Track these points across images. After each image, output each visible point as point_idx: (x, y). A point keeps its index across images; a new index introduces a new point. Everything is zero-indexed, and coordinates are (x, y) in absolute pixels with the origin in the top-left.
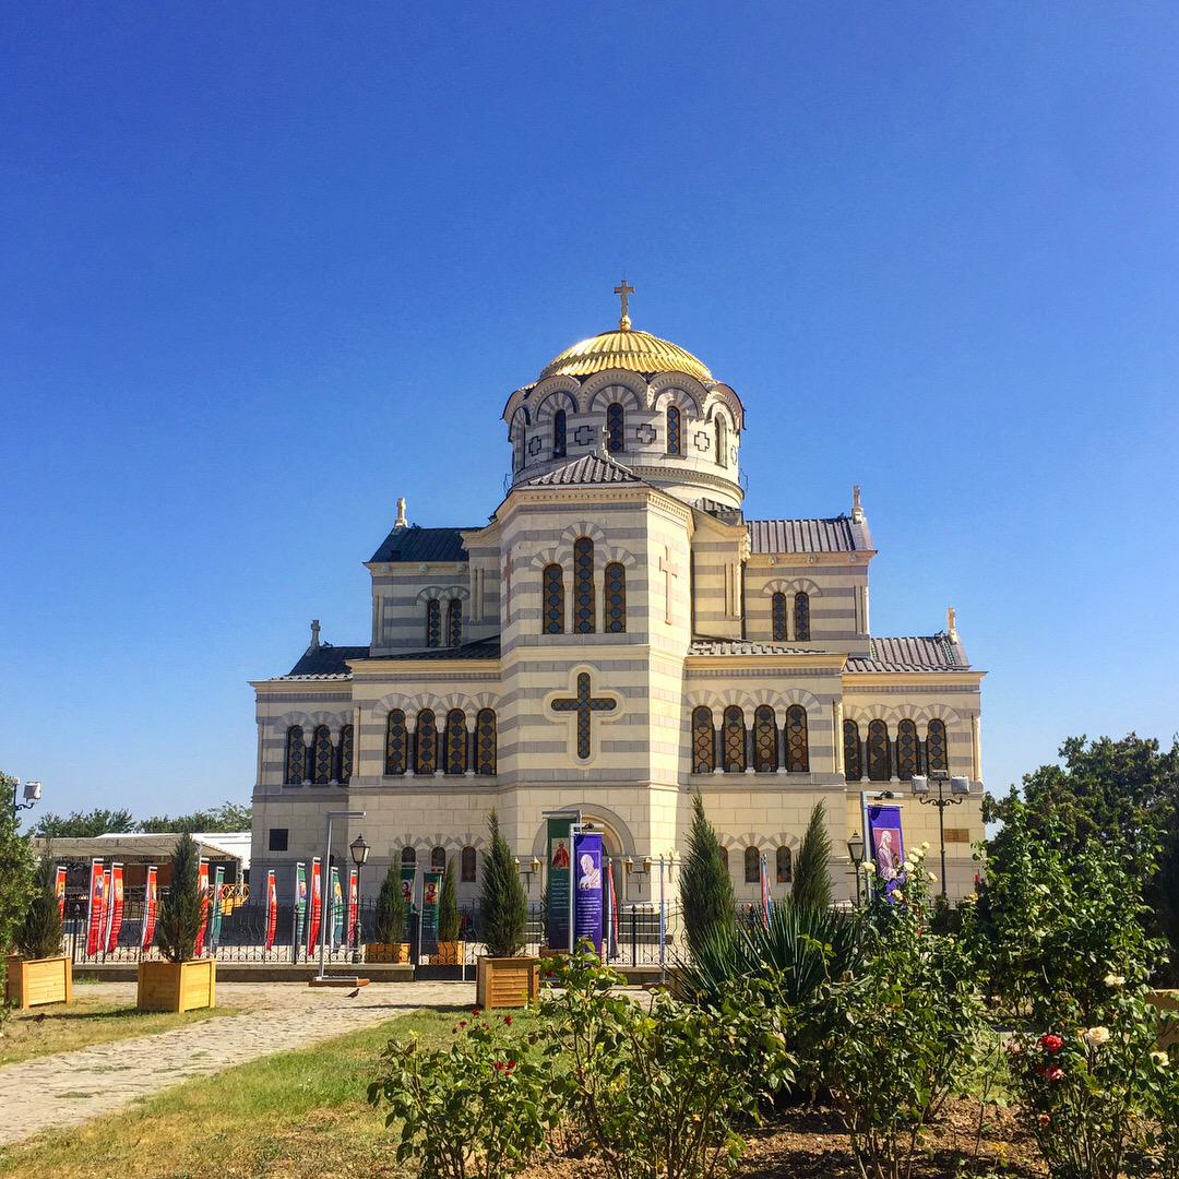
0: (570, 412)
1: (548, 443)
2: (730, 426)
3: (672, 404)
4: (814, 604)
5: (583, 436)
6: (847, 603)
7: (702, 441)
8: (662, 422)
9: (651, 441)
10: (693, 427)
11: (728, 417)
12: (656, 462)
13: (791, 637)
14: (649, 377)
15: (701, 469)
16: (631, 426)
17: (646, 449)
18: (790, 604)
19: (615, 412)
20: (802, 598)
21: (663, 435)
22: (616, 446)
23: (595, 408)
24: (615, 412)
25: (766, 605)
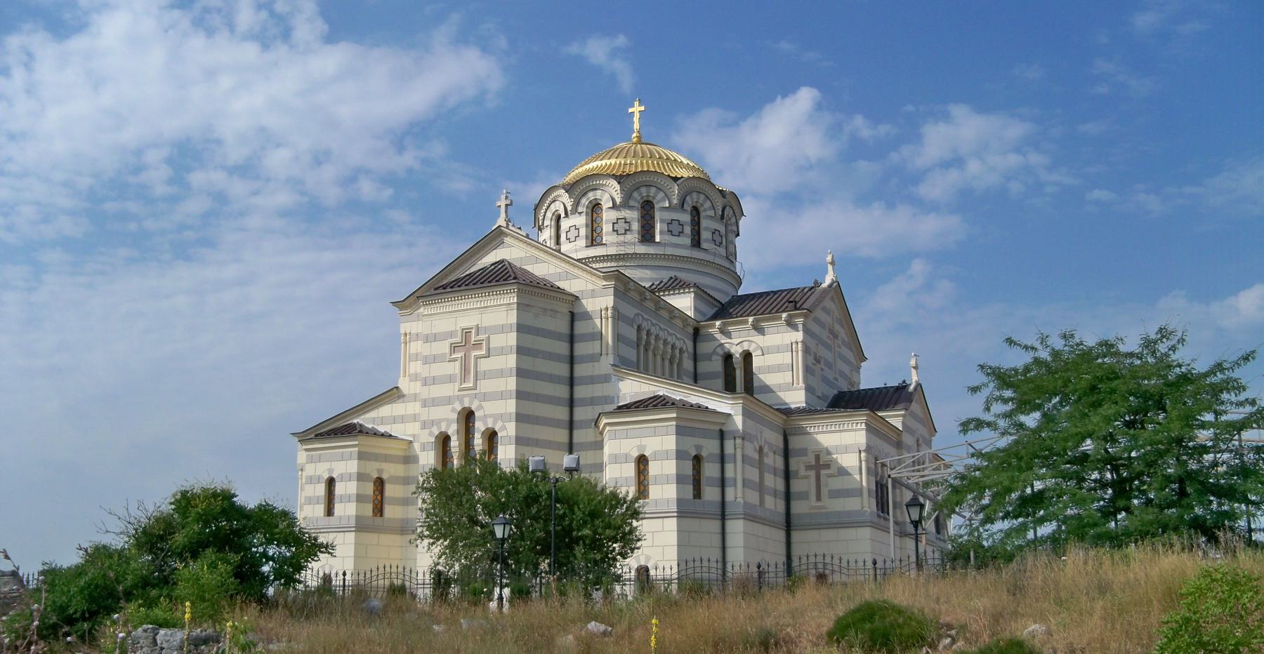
0: (563, 215)
2: (711, 213)
3: (645, 199)
4: (757, 362)
5: (572, 235)
6: (785, 358)
8: (633, 215)
11: (708, 204)
15: (669, 251)
16: (607, 222)
17: (621, 238)
20: (747, 356)
21: (636, 226)
23: (580, 209)
25: (717, 365)
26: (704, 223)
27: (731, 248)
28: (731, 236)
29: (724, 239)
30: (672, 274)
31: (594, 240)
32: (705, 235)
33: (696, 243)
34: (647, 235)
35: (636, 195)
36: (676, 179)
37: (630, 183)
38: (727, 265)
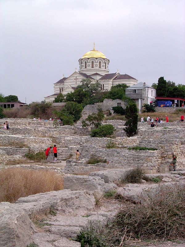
1: (80, 67)
7: (96, 66)
9: (90, 66)
10: (94, 64)
11: (102, 61)
12: (90, 69)
13: (102, 89)
14: (88, 58)
15: (96, 69)
17: (89, 67)
18: (102, 85)
19: (86, 62)
20: (103, 85)
21: (91, 65)
22: (86, 67)
24: (86, 62)
26: (101, 64)
27: (106, 67)
28: (107, 65)
29: (105, 66)
30: (96, 72)
31: (86, 67)
32: (102, 66)
33: (100, 67)
34: (93, 67)
35: (91, 61)
36: (97, 58)
37: (90, 59)
38: (105, 70)
